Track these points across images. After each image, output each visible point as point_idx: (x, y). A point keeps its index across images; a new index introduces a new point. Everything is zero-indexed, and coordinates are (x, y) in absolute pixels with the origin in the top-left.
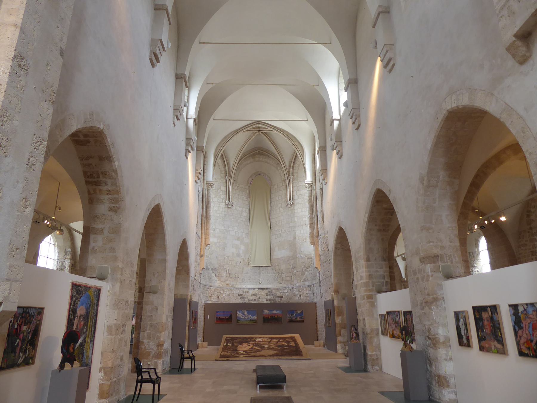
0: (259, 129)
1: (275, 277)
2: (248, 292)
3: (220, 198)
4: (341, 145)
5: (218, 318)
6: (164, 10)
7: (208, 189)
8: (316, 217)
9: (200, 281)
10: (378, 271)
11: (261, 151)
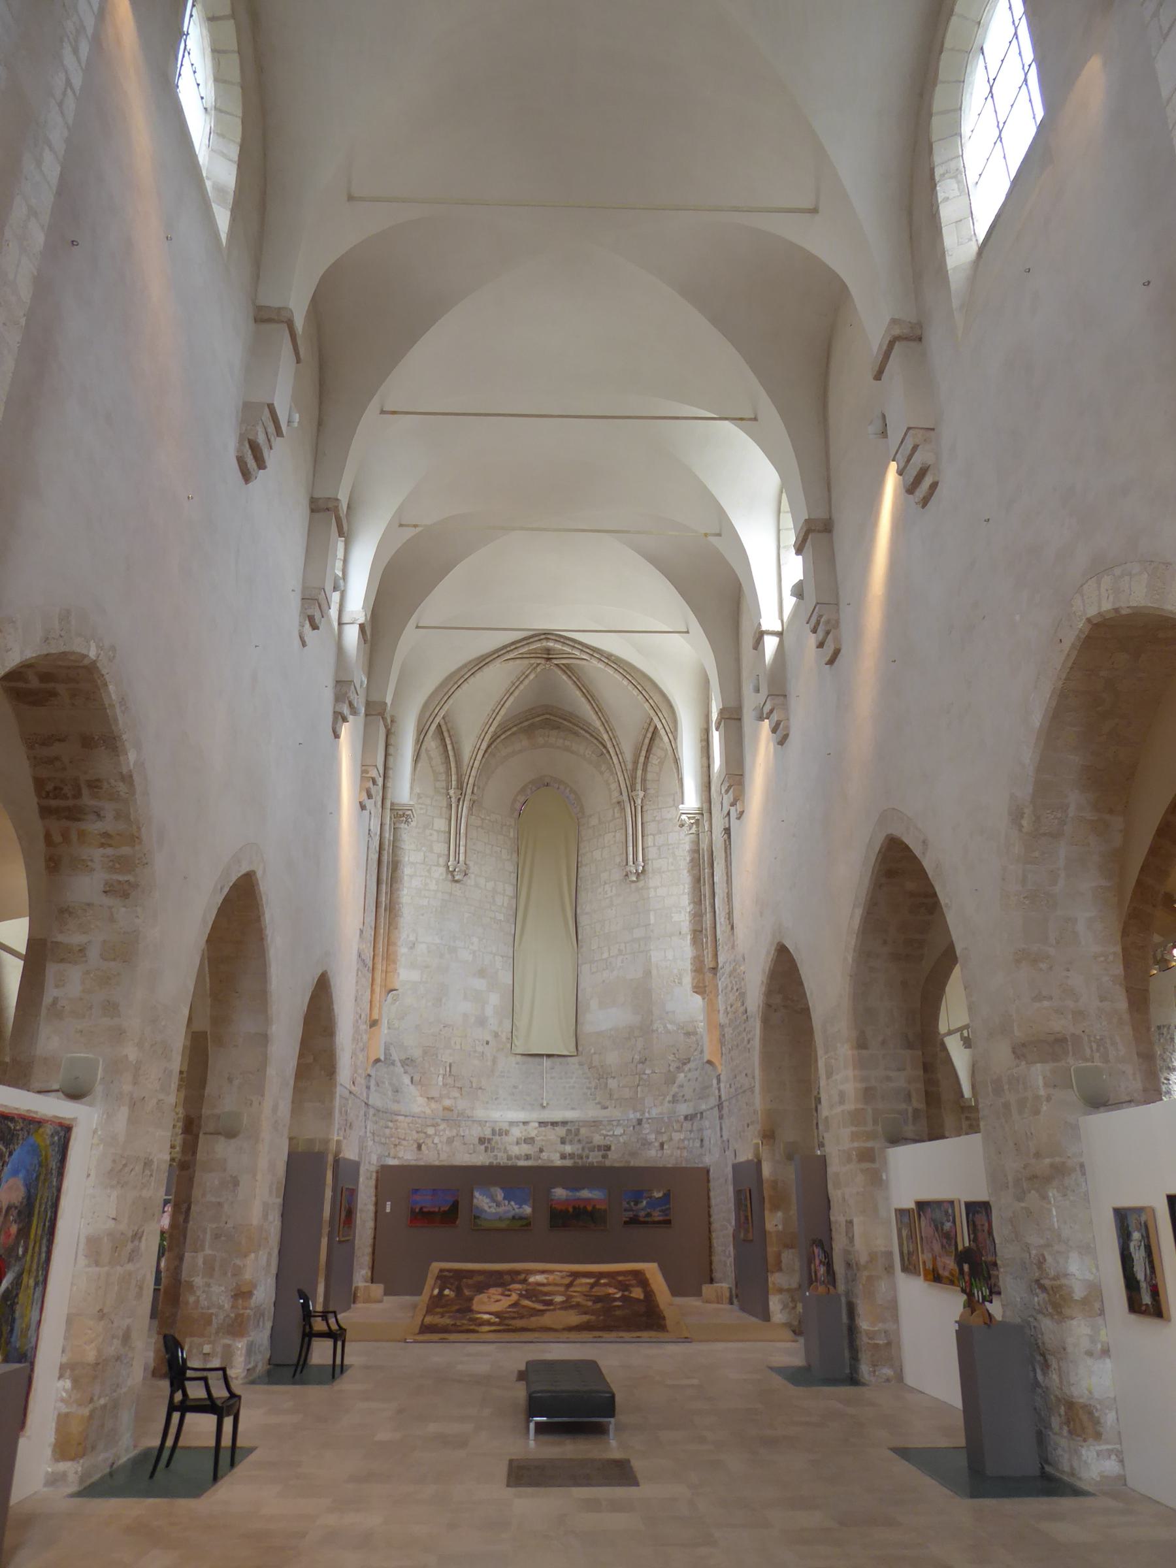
0: (549, 654)
2: (507, 1133)
3: (431, 851)
4: (785, 707)
5: (417, 1210)
6: (283, 322)
7: (397, 826)
8: (712, 914)
9: (368, 1098)
10: (888, 1079)
11: (552, 718)
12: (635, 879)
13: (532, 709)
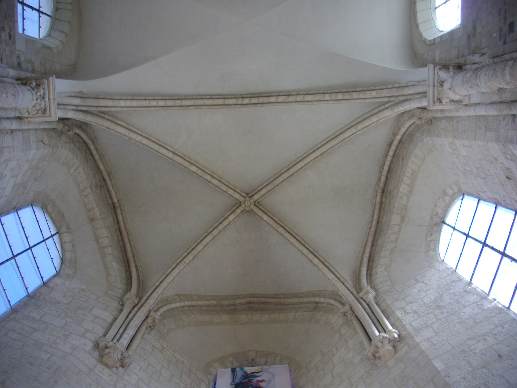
11: (255, 299)
13: (234, 295)
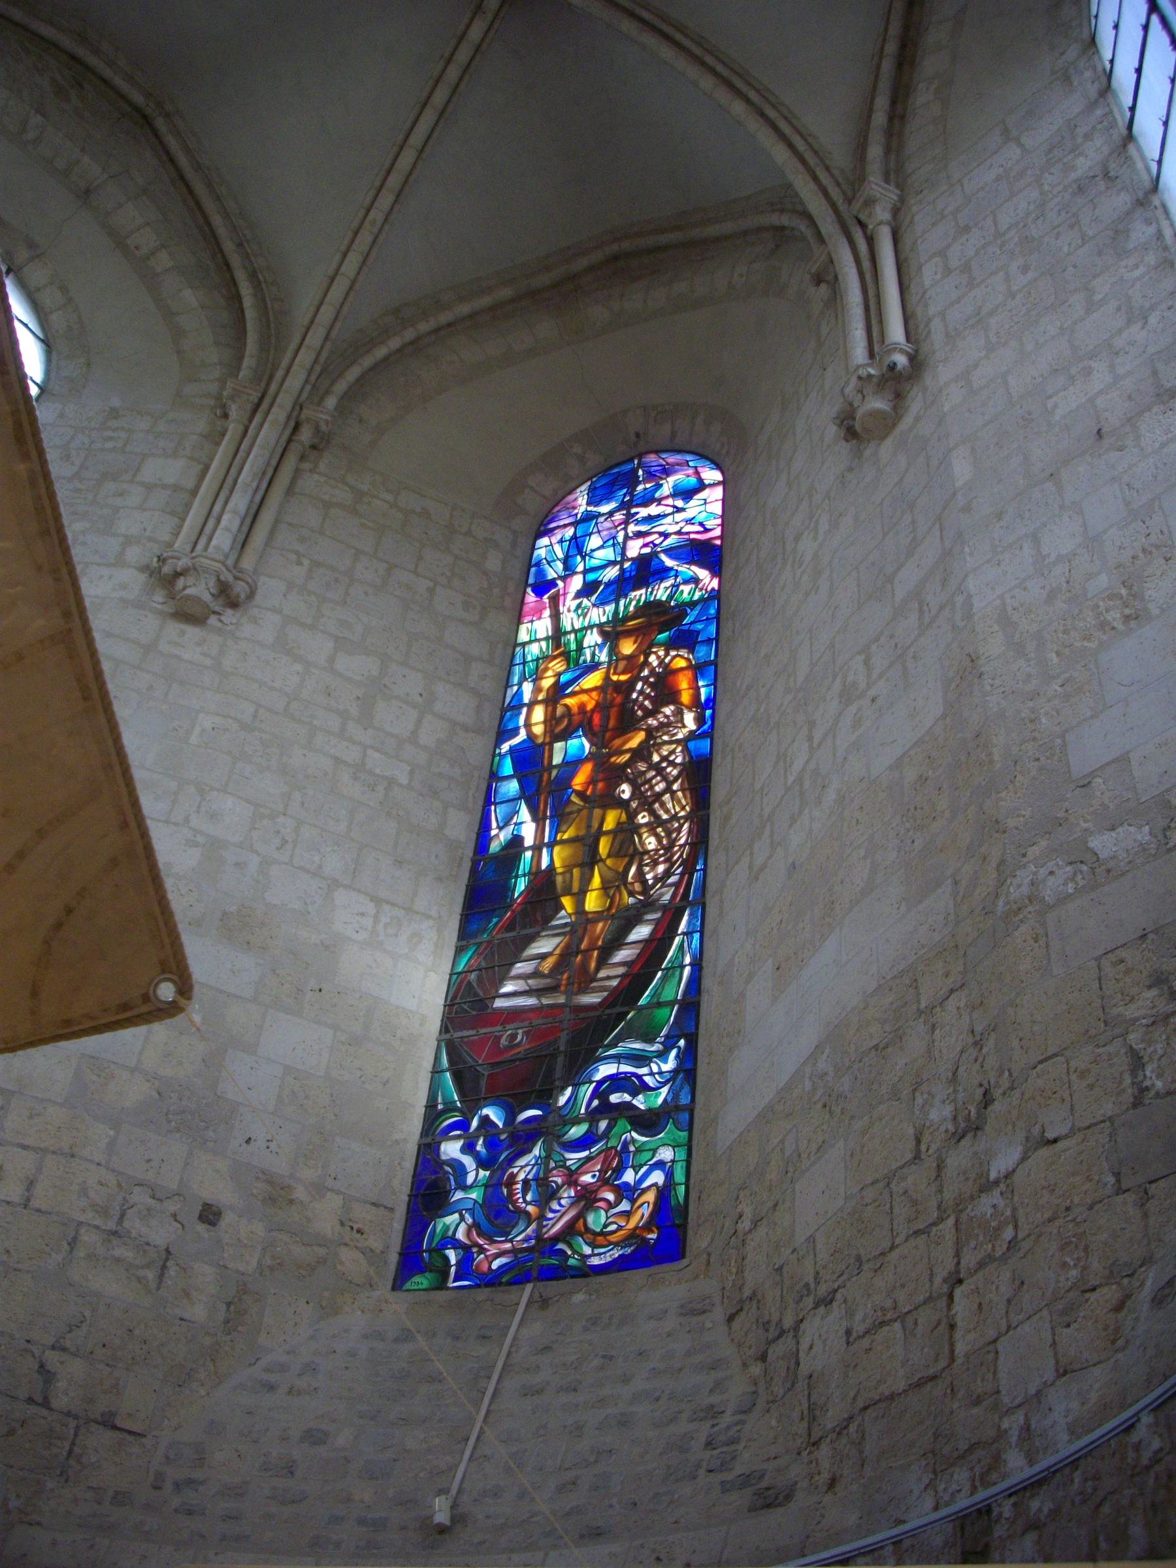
1: (713, 1412)
11: (626, 245)
12: (878, 404)
